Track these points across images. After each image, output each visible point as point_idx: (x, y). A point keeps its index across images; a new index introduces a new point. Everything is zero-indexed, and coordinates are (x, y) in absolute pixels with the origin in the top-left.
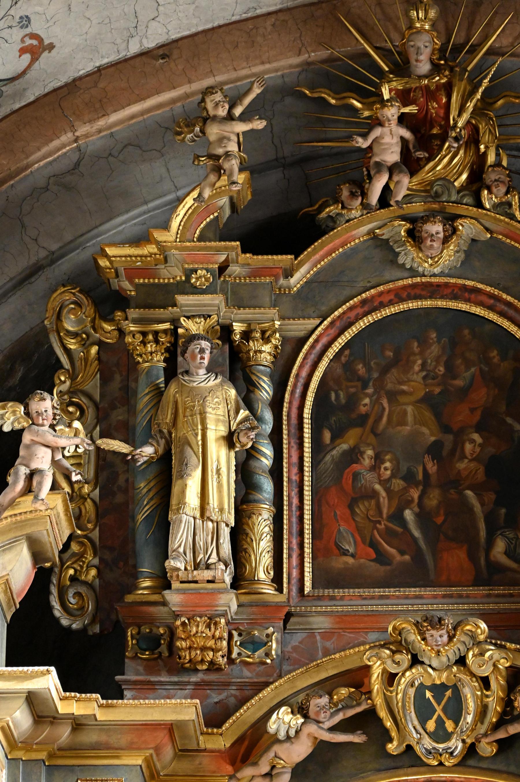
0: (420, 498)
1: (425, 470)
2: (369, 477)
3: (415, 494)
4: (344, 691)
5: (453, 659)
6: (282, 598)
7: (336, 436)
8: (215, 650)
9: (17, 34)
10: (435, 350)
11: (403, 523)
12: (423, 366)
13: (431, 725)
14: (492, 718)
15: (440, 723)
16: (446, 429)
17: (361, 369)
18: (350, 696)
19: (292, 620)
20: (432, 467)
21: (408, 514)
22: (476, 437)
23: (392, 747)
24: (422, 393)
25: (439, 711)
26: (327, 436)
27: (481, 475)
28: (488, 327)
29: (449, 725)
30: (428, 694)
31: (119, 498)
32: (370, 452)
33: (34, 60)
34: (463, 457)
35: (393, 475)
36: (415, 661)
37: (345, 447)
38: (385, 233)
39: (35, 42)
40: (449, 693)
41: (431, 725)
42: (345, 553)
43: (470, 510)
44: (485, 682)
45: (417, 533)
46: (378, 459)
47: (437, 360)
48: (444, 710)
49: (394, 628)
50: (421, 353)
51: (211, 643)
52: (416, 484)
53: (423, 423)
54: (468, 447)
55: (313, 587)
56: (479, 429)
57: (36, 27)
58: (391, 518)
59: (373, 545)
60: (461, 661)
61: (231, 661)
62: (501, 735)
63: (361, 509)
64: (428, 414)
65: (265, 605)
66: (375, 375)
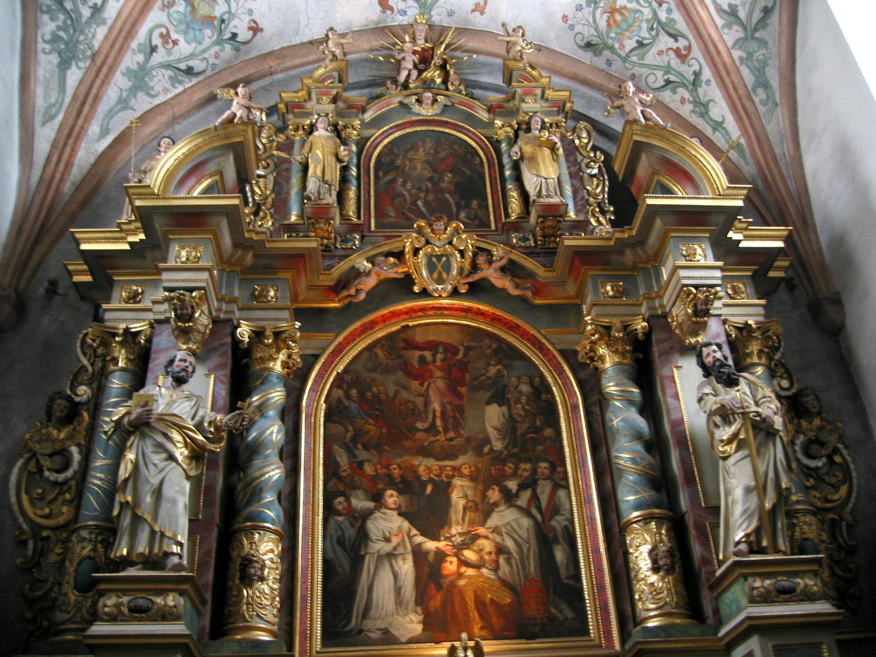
0: (425, 196)
1: (427, 187)
2: (400, 189)
3: (422, 195)
4: (392, 260)
5: (447, 241)
6: (360, 222)
7: (385, 174)
8: (329, 239)
9: (246, 18)
10: (429, 145)
11: (417, 206)
12: (424, 150)
13: (435, 275)
14: (466, 272)
15: (440, 274)
16: (435, 171)
17: (396, 151)
18: (394, 263)
19: (366, 238)
20: (429, 185)
21: (420, 203)
22: (449, 175)
23: (416, 289)
24: (424, 159)
25: (439, 268)
26: (381, 174)
27: (452, 189)
28: (452, 137)
29: (444, 275)
30: (434, 259)
31: (284, 196)
32: (401, 180)
33: (255, 34)
34: (443, 182)
35: (412, 188)
36: (428, 242)
37: (389, 178)
38: (406, 101)
39: (254, 25)
40: (444, 259)
41: (435, 275)
42: (390, 217)
43: (448, 201)
44: (462, 253)
45: (423, 209)
46: (404, 183)
47: (430, 148)
48: (442, 267)
49: (418, 226)
50: (423, 146)
51: (326, 235)
52: (423, 191)
53: (425, 169)
54: (446, 178)
55: (376, 227)
56: (450, 172)
57: (256, 17)
58: (411, 204)
59: (403, 214)
60: (450, 243)
61: (336, 248)
62: (470, 280)
63: (397, 200)
64: (427, 166)
65: (355, 225)
66: (403, 153)
